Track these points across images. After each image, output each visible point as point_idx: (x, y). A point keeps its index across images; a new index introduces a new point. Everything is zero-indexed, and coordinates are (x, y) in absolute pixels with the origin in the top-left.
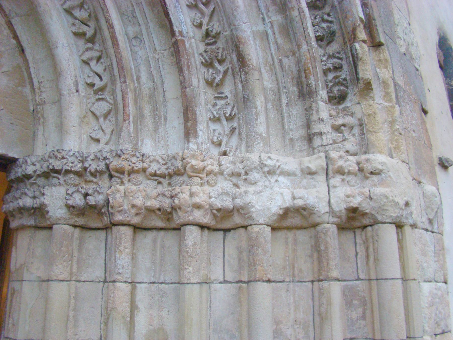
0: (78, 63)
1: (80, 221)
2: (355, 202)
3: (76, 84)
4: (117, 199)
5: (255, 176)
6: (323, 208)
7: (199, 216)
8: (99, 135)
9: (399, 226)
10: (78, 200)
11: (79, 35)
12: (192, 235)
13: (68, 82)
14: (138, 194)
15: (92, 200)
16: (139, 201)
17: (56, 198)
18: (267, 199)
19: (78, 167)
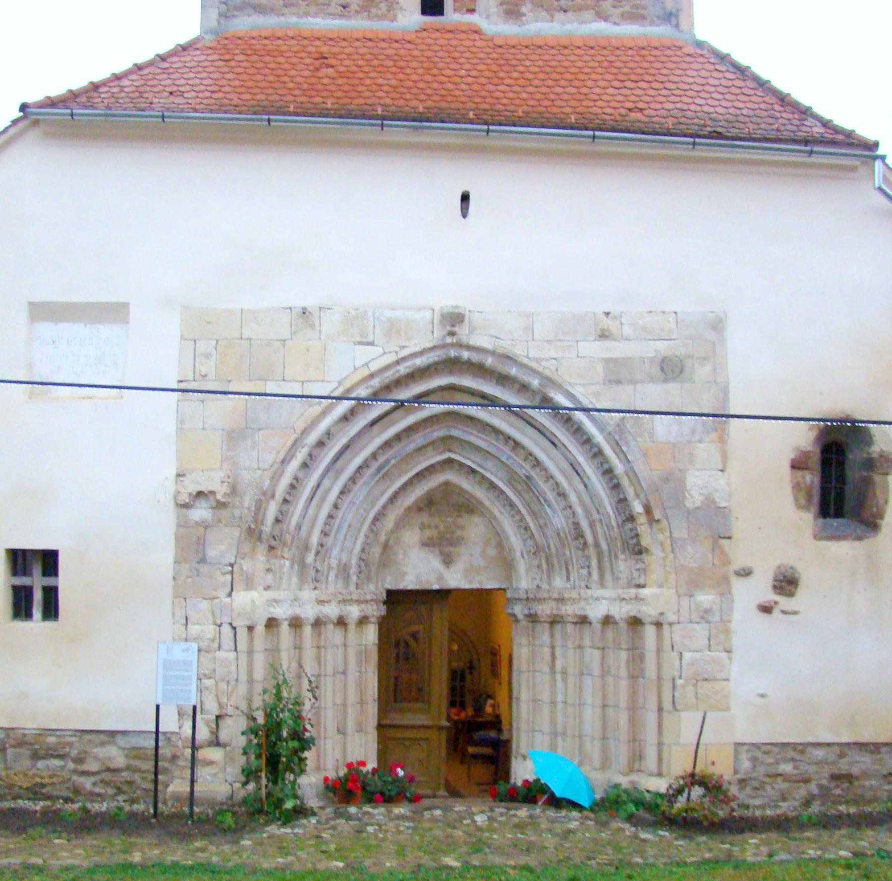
0: (521, 543)
1: (531, 619)
2: (632, 614)
3: (522, 554)
4: (539, 612)
5: (591, 601)
6: (617, 617)
7: (570, 619)
8: (536, 576)
9: (658, 625)
10: (526, 612)
11: (520, 527)
12: (570, 628)
13: (518, 554)
14: (545, 610)
15: (533, 612)
16: (548, 612)
17: (519, 610)
18: (596, 612)
19: (525, 597)
